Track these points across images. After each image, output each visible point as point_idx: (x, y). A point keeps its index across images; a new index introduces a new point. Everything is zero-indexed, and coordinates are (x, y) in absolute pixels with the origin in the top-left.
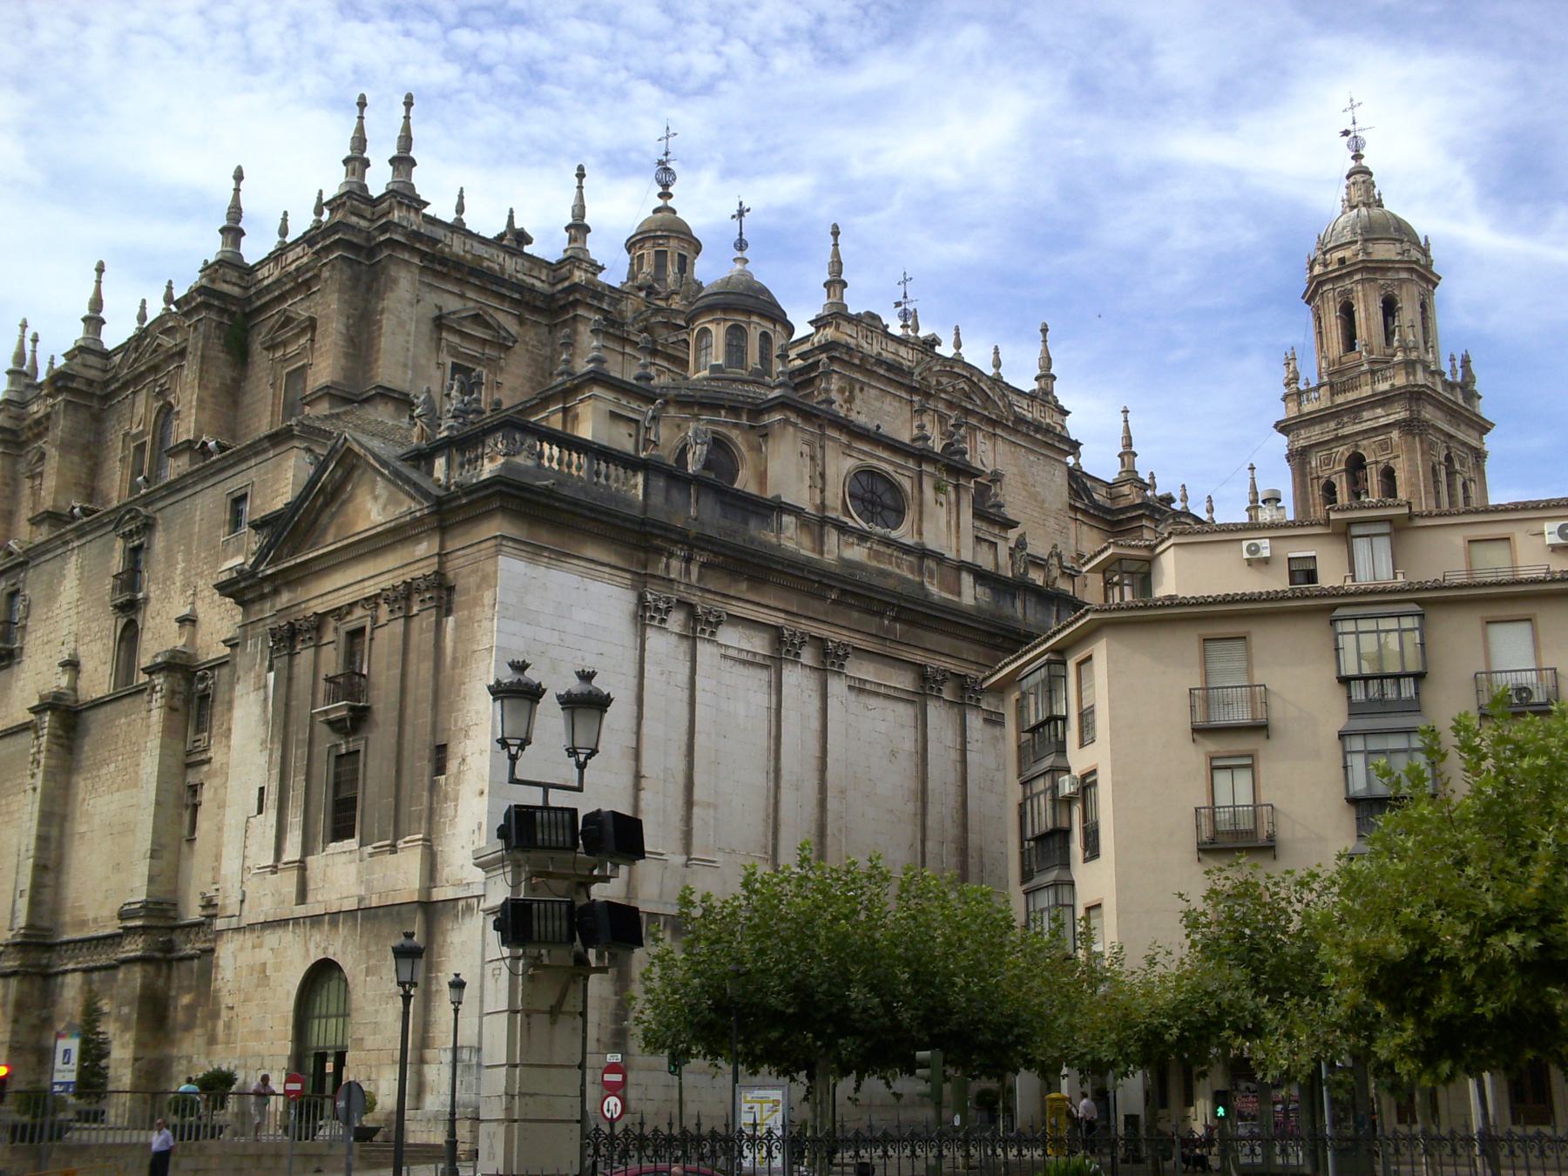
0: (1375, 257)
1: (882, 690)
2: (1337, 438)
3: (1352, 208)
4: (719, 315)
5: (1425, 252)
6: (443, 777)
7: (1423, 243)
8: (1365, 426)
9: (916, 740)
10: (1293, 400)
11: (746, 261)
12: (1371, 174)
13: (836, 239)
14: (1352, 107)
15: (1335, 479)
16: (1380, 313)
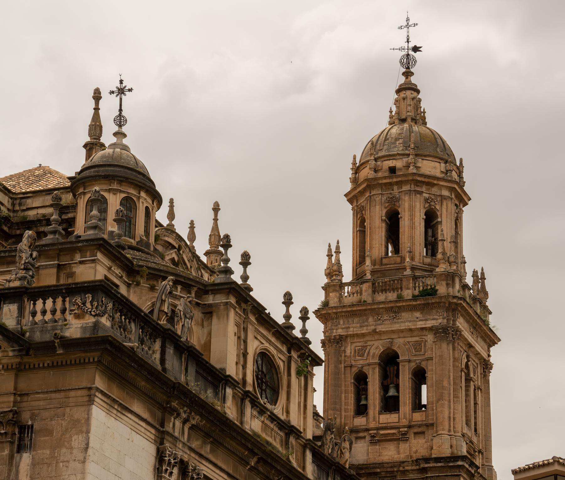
3: (403, 121)
4: (115, 186)
5: (460, 170)
7: (458, 164)
8: (403, 326)
10: (335, 291)
11: (125, 135)
12: (418, 92)
13: (97, 103)
14: (408, 26)
16: (423, 224)
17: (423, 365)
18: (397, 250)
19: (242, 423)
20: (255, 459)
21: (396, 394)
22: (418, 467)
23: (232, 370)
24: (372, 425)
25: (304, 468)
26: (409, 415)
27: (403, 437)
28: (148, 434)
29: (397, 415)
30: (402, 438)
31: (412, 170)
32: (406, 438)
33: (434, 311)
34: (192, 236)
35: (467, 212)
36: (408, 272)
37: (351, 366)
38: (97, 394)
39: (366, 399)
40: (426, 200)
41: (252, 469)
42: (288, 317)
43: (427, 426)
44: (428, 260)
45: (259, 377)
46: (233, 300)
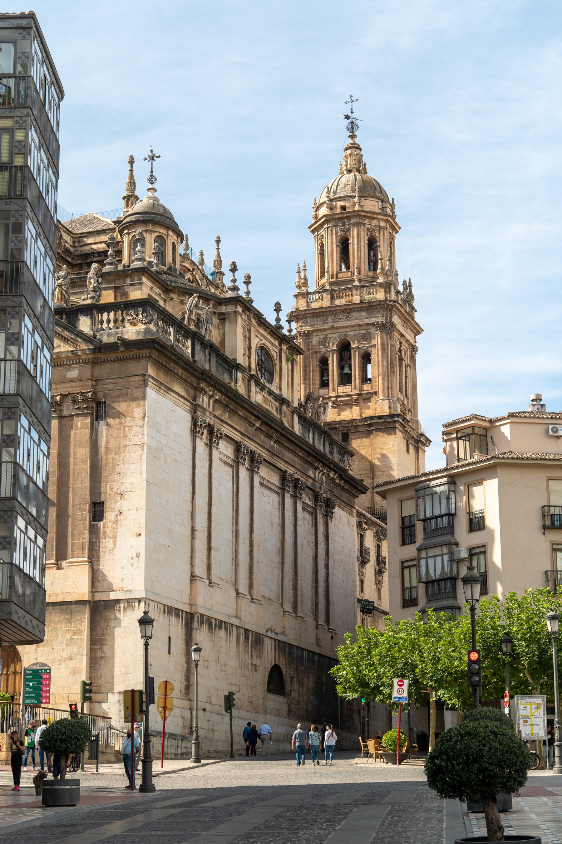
0: (365, 209)
1: (269, 485)
4: (150, 227)
6: (102, 523)
7: (391, 202)
8: (354, 323)
9: (279, 517)
11: (155, 190)
12: (360, 149)
13: (132, 166)
14: (352, 101)
18: (348, 268)
19: (249, 397)
20: (260, 422)
21: (349, 372)
23: (241, 360)
24: (332, 394)
25: (293, 427)
28: (186, 406)
31: (357, 208)
34: (202, 262)
35: (399, 238)
36: (356, 283)
38: (149, 379)
40: (368, 230)
41: (258, 429)
42: (278, 320)
44: (371, 274)
45: (260, 365)
46: (240, 309)
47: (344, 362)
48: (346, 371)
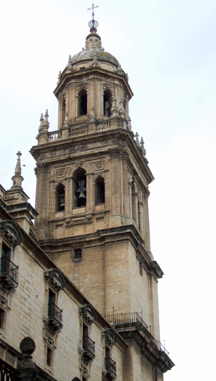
2: (70, 159)
8: (89, 152)
12: (100, 38)
14: (93, 8)
15: (64, 183)
17: (103, 175)
21: (84, 197)
22: (98, 237)
26: (93, 207)
27: (89, 221)
29: (84, 209)
30: (88, 222)
32: (91, 221)
33: (109, 141)
37: (54, 182)
39: (64, 202)
40: (104, 85)
43: (105, 212)
47: (80, 190)
48: (82, 195)
